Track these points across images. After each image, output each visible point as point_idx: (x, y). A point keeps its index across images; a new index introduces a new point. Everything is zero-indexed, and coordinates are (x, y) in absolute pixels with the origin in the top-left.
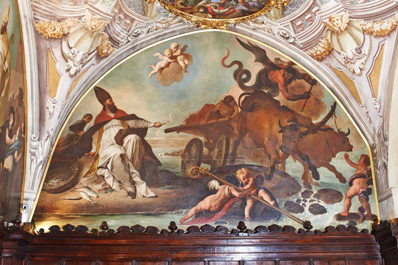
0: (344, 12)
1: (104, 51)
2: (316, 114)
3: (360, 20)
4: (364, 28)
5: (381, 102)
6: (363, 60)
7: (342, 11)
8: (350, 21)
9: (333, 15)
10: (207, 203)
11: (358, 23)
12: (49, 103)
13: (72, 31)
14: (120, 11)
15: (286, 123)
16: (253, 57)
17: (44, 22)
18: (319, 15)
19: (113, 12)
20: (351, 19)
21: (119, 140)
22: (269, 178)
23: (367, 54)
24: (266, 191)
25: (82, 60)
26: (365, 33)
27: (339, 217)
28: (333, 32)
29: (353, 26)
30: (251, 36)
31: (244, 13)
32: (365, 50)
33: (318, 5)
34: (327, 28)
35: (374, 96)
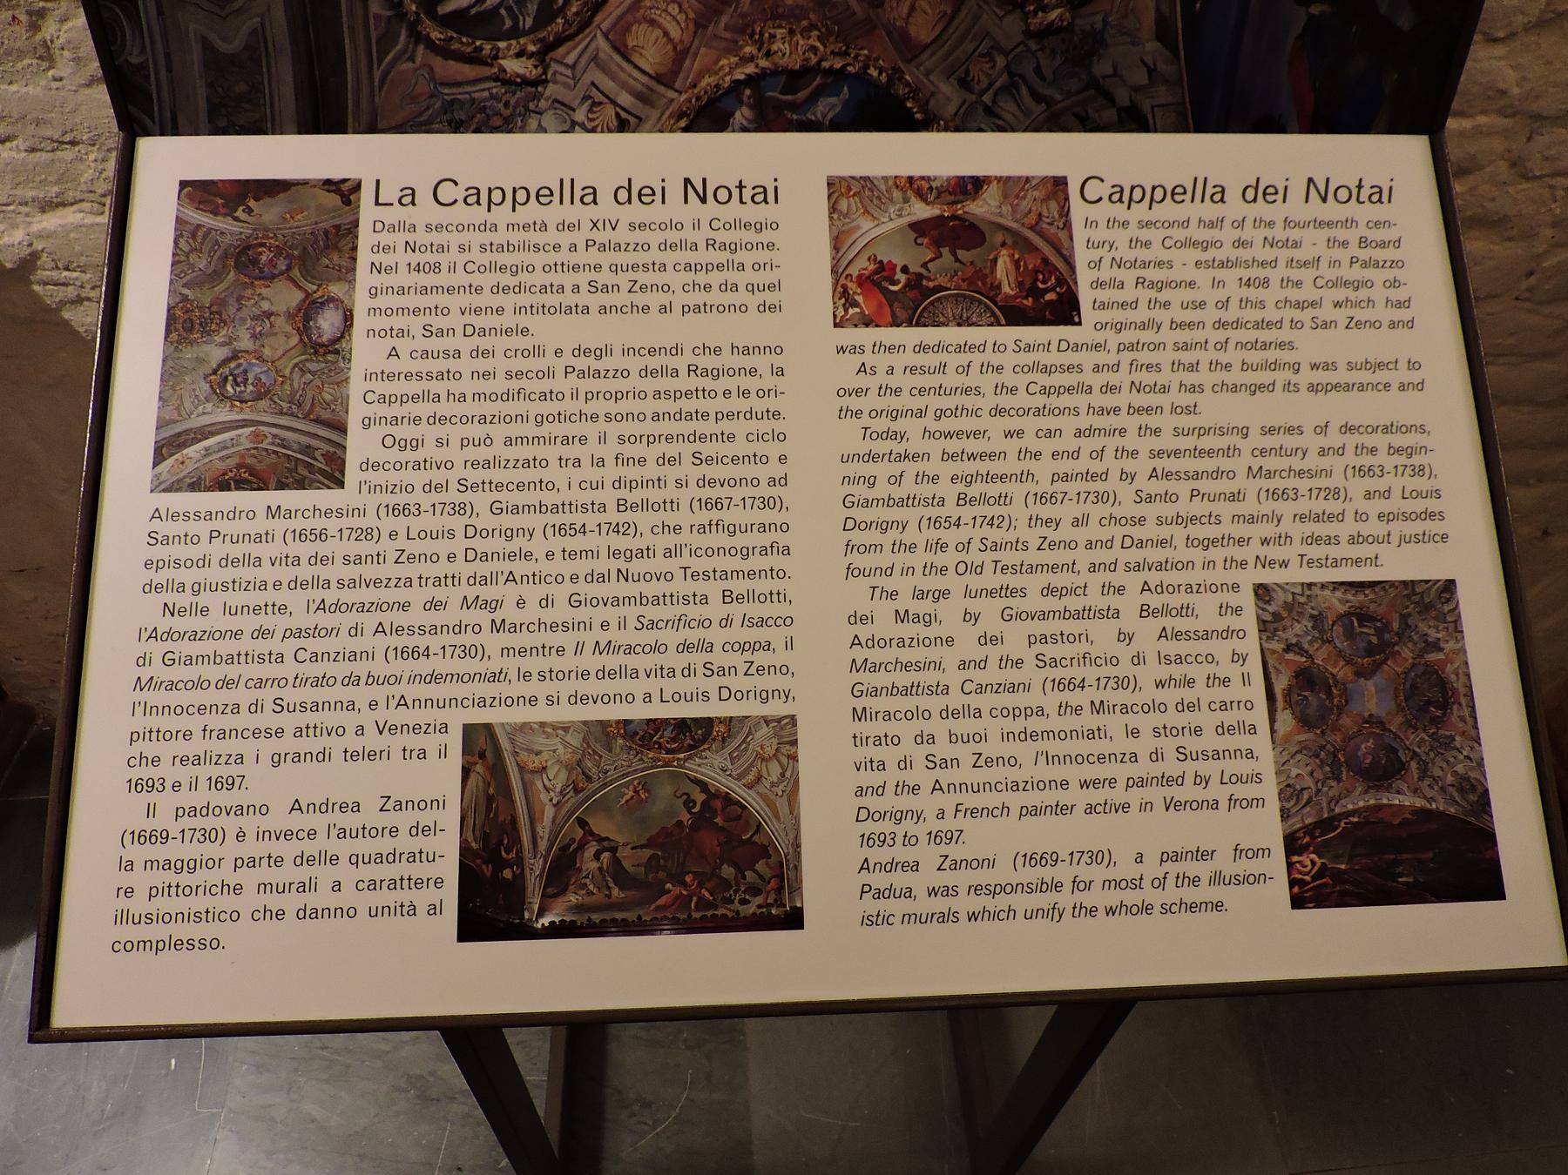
1: (581, 785)
2: (745, 832)
10: (662, 901)
12: (539, 829)
13: (549, 764)
14: (589, 746)
15: (722, 839)
16: (698, 789)
17: (523, 755)
19: (582, 746)
21: (597, 856)
22: (709, 880)
24: (707, 890)
25: (561, 791)
27: (759, 906)
30: (696, 772)
31: (691, 748)
35: (791, 813)
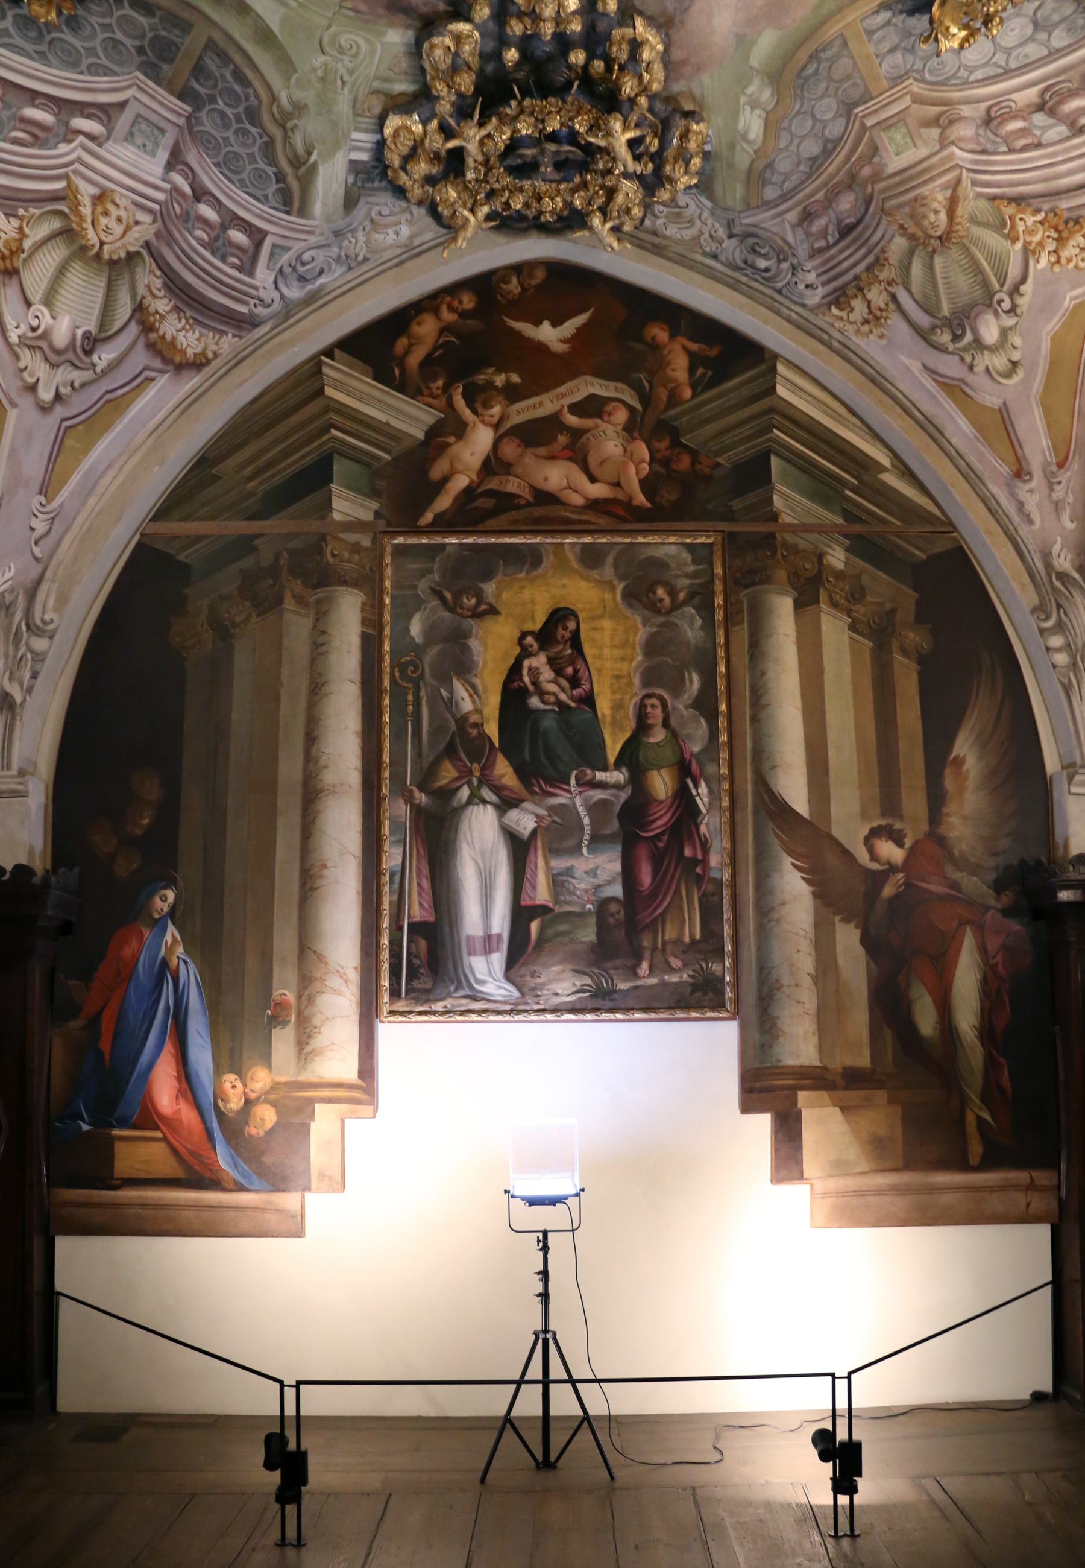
0: (146, 218)
3: (158, 273)
4: (148, 300)
5: (57, 521)
6: (78, 377)
7: (150, 211)
8: (138, 253)
9: (123, 198)
11: (148, 278)
18: (80, 152)
20: (144, 252)
23: (98, 370)
26: (137, 315)
28: (68, 233)
29: (132, 274)
32: (104, 357)
33: (109, 124)
34: (62, 207)
35: (46, 489)
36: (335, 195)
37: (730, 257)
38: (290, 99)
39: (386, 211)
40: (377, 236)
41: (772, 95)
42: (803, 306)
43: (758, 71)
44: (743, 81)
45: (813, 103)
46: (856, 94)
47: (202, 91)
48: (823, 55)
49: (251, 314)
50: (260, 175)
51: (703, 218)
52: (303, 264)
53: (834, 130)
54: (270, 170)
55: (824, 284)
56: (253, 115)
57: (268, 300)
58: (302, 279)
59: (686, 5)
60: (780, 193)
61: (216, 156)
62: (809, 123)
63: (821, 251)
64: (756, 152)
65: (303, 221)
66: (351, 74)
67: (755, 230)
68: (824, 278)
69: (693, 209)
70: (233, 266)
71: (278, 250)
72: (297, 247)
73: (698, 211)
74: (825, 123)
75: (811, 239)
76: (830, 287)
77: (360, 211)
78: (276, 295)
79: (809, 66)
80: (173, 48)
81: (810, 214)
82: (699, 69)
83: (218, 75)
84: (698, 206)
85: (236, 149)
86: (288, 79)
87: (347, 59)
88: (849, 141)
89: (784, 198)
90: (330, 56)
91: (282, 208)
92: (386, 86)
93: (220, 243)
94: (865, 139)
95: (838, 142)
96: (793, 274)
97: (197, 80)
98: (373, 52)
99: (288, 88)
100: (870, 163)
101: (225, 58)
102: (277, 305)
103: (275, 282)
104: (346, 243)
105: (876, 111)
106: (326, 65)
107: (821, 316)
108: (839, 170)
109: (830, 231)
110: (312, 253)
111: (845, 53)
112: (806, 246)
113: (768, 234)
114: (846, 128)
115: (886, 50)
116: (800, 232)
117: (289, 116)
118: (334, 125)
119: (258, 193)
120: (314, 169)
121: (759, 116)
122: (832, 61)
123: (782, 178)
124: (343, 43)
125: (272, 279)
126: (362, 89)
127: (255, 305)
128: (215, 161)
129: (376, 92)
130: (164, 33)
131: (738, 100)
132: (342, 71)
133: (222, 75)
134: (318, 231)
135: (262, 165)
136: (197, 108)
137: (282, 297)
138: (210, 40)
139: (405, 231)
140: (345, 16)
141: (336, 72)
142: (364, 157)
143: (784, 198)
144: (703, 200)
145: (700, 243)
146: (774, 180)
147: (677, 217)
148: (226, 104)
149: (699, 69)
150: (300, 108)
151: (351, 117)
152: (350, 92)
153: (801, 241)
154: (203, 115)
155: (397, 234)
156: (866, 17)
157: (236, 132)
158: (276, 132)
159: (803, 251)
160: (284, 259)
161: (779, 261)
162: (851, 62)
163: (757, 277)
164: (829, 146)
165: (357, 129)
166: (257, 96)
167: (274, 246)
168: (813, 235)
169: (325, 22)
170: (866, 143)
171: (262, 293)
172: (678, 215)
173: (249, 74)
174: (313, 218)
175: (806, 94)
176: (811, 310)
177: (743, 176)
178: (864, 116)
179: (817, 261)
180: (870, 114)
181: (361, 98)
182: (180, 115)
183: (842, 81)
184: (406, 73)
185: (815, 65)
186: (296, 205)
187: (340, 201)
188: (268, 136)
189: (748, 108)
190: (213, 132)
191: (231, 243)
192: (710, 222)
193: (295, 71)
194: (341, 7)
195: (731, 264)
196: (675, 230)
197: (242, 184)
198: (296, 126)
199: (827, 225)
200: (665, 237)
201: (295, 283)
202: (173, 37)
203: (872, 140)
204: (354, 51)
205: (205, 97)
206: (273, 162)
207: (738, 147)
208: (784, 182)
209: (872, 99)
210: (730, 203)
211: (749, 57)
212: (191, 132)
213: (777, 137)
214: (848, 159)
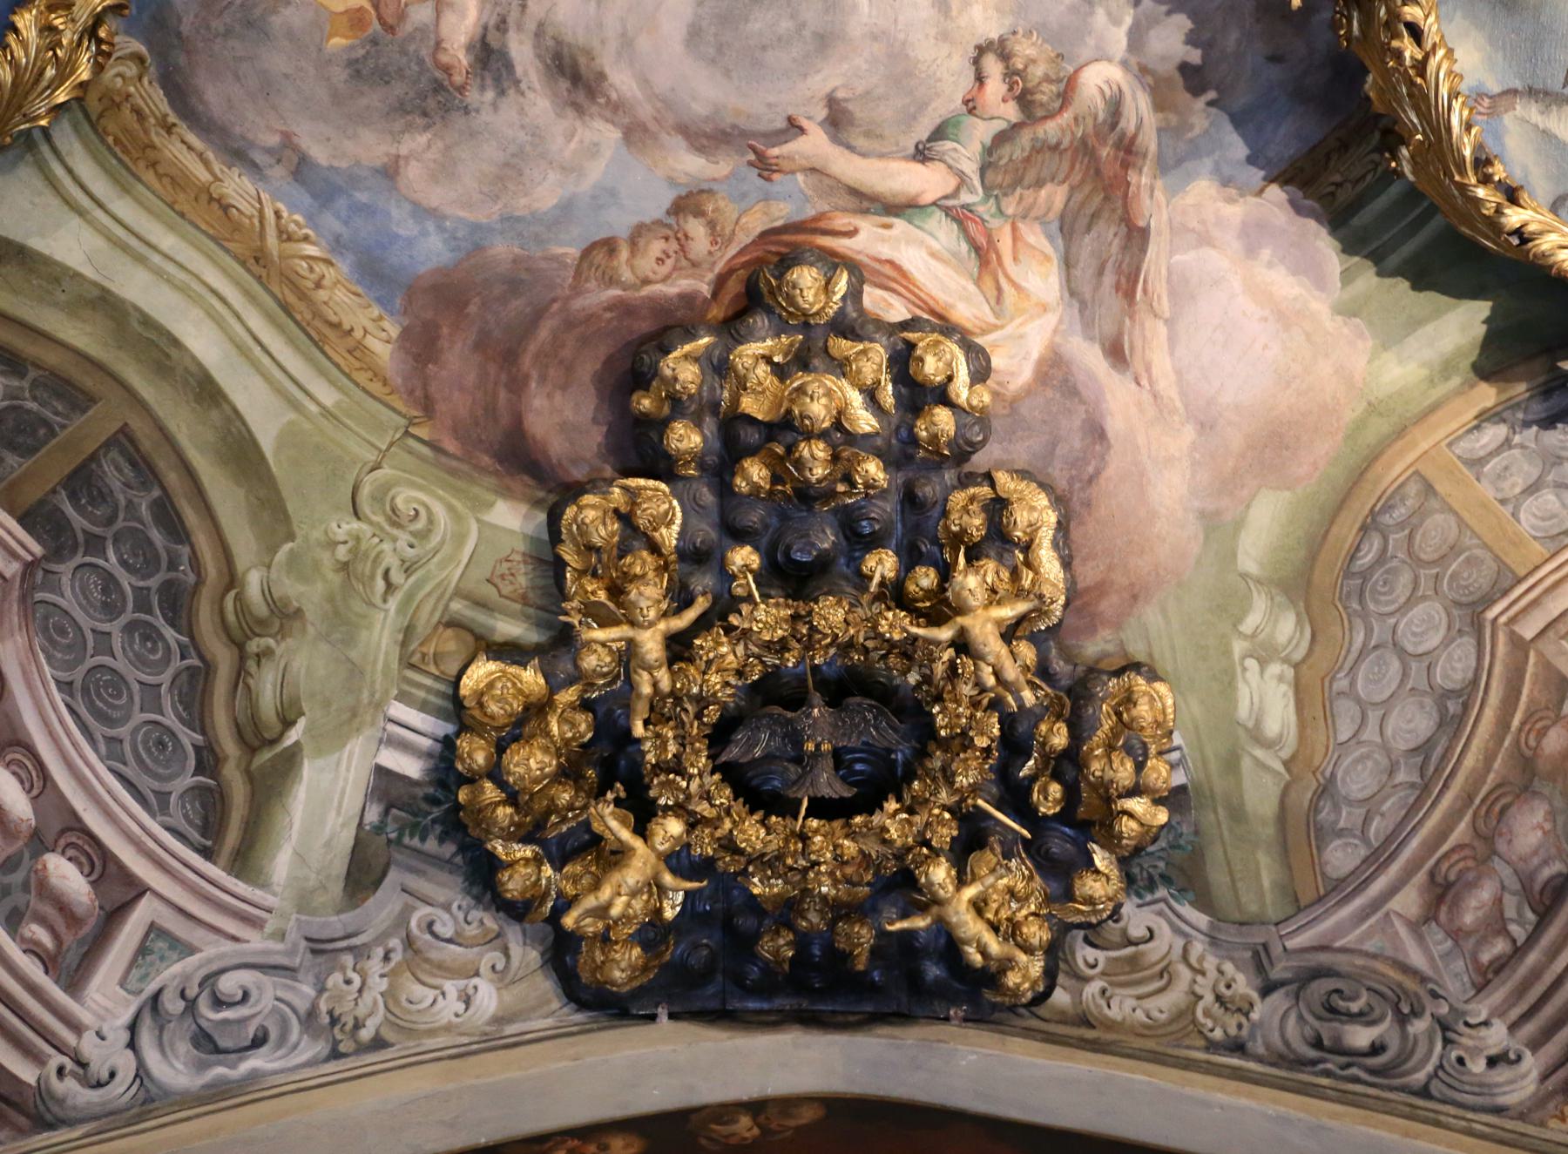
36: (328, 844)
37: (1276, 1039)
38: (267, 592)
39: (446, 930)
40: (418, 990)
41: (1299, 622)
42: (1499, 1110)
43: (1259, 581)
44: (1229, 606)
45: (1392, 621)
46: (1481, 579)
47: (78, 521)
48: (1386, 519)
49: (41, 1090)
50: (162, 740)
51: (1193, 960)
52: (219, 1003)
53: (1455, 666)
54: (189, 738)
55: (1535, 1045)
56: (177, 603)
57: (99, 1069)
58: (205, 1042)
59: (1091, 469)
60: (1363, 852)
61: (70, 666)
62: (1395, 665)
63: (1500, 966)
64: (1286, 764)
65: (240, 887)
66: (408, 571)
67: (1324, 958)
68: (1530, 1028)
69: (1166, 942)
70: (33, 949)
71: (161, 944)
72: (212, 951)
73: (1179, 943)
74: (1428, 659)
75: (1469, 944)
76: (1552, 1049)
77: (384, 905)
78: (125, 1064)
79: (1365, 547)
80: (42, 432)
81: (1448, 886)
82: (1135, 597)
83: (123, 502)
84: (1177, 931)
85: (121, 664)
86: (273, 550)
87: (404, 538)
88: (1494, 684)
89: (1378, 859)
90: (371, 523)
91: (195, 836)
92: (481, 617)
93: (17, 878)
94: (1530, 669)
95: (1468, 693)
96: (1447, 1042)
97: (74, 497)
98: (460, 539)
99: (269, 567)
100: (1558, 718)
101: (145, 471)
102: (119, 1091)
103: (133, 1028)
104: (335, 979)
105: (1535, 603)
106: (358, 539)
107: (1553, 1123)
108: (1489, 759)
109: (1510, 912)
110: (246, 977)
111: (1434, 504)
112: (1459, 965)
113: (1360, 961)
114: (1480, 658)
115: (1518, 490)
116: (1439, 941)
117: (258, 626)
118: (355, 672)
119: (146, 783)
120: (291, 759)
121: (1281, 679)
122: (1411, 526)
123: (1360, 812)
124: (399, 502)
125: (126, 1016)
126: (427, 607)
127: (61, 1071)
128: (64, 676)
129: (453, 623)
130: (32, 405)
131: (1228, 653)
132: (390, 560)
133: (130, 503)
134: (272, 924)
135: (170, 720)
136: (57, 553)
137: (142, 1073)
138: (124, 430)
139: (488, 998)
140: (411, 452)
141: (377, 560)
142: (411, 767)
143: (1378, 859)
144: (1187, 911)
145: (1194, 1021)
146: (1342, 824)
147: (1130, 970)
148: (123, 563)
149: (1135, 597)
150: (284, 616)
151: (395, 665)
152: (401, 610)
153: (1446, 956)
154: (65, 569)
155: (467, 1001)
156: (1459, 438)
157: (130, 628)
158: (223, 657)
159: (1455, 981)
160: (171, 973)
161: (1402, 1020)
162: (1452, 520)
163: (1354, 1071)
164: (1453, 707)
165: (403, 697)
166: (196, 563)
167: (154, 930)
168: (1469, 934)
169: (372, 456)
170: (1535, 664)
171: (88, 1046)
172: (1134, 962)
173: (191, 517)
174: (265, 886)
175: (1372, 606)
176: (1522, 1117)
177: (1270, 831)
178: (1513, 620)
179: (1498, 995)
180: (1524, 610)
181: (422, 628)
182: (13, 555)
183: (1442, 560)
184: (524, 600)
185: (1377, 543)
186: (232, 837)
187: (340, 866)
188: (201, 657)
189: (1252, 664)
190: (78, 615)
191: (46, 891)
192: (1210, 963)
193: (291, 537)
194: (407, 433)
195: (1281, 1056)
196: (1131, 1002)
197: (113, 752)
198: (268, 653)
199: (1498, 901)
200: (1110, 1025)
201: (184, 1047)
202: (48, 414)
203: (1546, 665)
204: (420, 525)
205: (81, 537)
206: (198, 717)
207: (1246, 764)
208: (1367, 821)
209: (1520, 581)
210: (1253, 908)
211: (1234, 555)
212: (23, 598)
213: (1330, 718)
214: (1503, 723)
